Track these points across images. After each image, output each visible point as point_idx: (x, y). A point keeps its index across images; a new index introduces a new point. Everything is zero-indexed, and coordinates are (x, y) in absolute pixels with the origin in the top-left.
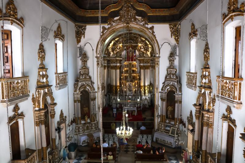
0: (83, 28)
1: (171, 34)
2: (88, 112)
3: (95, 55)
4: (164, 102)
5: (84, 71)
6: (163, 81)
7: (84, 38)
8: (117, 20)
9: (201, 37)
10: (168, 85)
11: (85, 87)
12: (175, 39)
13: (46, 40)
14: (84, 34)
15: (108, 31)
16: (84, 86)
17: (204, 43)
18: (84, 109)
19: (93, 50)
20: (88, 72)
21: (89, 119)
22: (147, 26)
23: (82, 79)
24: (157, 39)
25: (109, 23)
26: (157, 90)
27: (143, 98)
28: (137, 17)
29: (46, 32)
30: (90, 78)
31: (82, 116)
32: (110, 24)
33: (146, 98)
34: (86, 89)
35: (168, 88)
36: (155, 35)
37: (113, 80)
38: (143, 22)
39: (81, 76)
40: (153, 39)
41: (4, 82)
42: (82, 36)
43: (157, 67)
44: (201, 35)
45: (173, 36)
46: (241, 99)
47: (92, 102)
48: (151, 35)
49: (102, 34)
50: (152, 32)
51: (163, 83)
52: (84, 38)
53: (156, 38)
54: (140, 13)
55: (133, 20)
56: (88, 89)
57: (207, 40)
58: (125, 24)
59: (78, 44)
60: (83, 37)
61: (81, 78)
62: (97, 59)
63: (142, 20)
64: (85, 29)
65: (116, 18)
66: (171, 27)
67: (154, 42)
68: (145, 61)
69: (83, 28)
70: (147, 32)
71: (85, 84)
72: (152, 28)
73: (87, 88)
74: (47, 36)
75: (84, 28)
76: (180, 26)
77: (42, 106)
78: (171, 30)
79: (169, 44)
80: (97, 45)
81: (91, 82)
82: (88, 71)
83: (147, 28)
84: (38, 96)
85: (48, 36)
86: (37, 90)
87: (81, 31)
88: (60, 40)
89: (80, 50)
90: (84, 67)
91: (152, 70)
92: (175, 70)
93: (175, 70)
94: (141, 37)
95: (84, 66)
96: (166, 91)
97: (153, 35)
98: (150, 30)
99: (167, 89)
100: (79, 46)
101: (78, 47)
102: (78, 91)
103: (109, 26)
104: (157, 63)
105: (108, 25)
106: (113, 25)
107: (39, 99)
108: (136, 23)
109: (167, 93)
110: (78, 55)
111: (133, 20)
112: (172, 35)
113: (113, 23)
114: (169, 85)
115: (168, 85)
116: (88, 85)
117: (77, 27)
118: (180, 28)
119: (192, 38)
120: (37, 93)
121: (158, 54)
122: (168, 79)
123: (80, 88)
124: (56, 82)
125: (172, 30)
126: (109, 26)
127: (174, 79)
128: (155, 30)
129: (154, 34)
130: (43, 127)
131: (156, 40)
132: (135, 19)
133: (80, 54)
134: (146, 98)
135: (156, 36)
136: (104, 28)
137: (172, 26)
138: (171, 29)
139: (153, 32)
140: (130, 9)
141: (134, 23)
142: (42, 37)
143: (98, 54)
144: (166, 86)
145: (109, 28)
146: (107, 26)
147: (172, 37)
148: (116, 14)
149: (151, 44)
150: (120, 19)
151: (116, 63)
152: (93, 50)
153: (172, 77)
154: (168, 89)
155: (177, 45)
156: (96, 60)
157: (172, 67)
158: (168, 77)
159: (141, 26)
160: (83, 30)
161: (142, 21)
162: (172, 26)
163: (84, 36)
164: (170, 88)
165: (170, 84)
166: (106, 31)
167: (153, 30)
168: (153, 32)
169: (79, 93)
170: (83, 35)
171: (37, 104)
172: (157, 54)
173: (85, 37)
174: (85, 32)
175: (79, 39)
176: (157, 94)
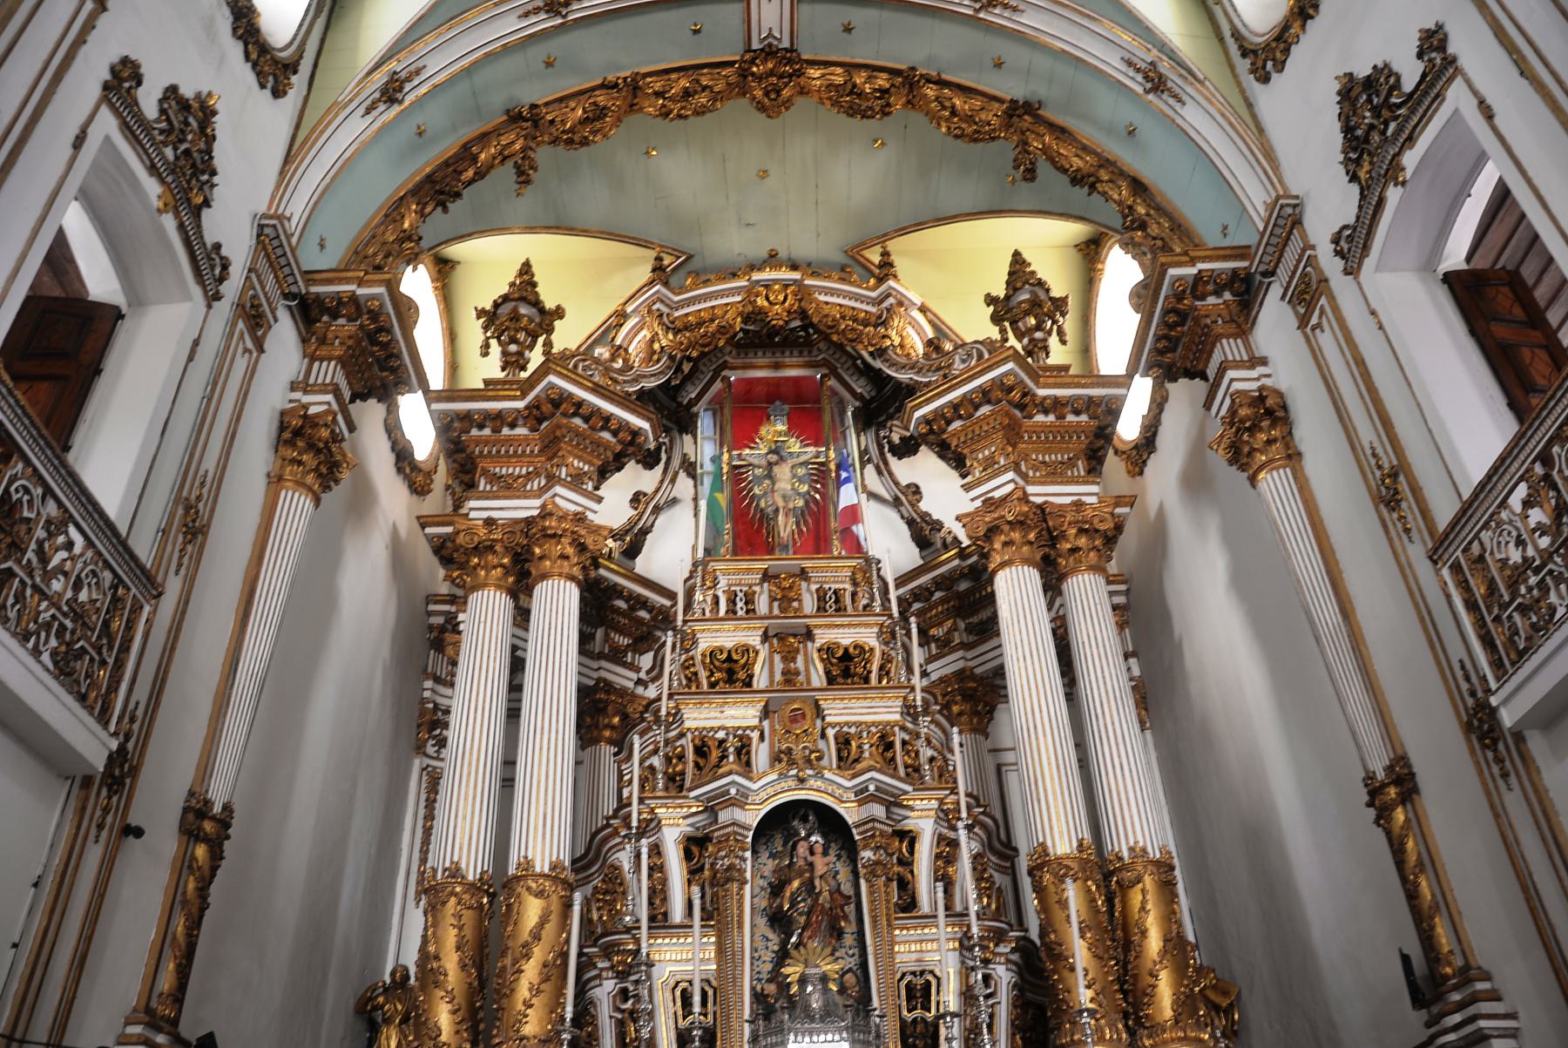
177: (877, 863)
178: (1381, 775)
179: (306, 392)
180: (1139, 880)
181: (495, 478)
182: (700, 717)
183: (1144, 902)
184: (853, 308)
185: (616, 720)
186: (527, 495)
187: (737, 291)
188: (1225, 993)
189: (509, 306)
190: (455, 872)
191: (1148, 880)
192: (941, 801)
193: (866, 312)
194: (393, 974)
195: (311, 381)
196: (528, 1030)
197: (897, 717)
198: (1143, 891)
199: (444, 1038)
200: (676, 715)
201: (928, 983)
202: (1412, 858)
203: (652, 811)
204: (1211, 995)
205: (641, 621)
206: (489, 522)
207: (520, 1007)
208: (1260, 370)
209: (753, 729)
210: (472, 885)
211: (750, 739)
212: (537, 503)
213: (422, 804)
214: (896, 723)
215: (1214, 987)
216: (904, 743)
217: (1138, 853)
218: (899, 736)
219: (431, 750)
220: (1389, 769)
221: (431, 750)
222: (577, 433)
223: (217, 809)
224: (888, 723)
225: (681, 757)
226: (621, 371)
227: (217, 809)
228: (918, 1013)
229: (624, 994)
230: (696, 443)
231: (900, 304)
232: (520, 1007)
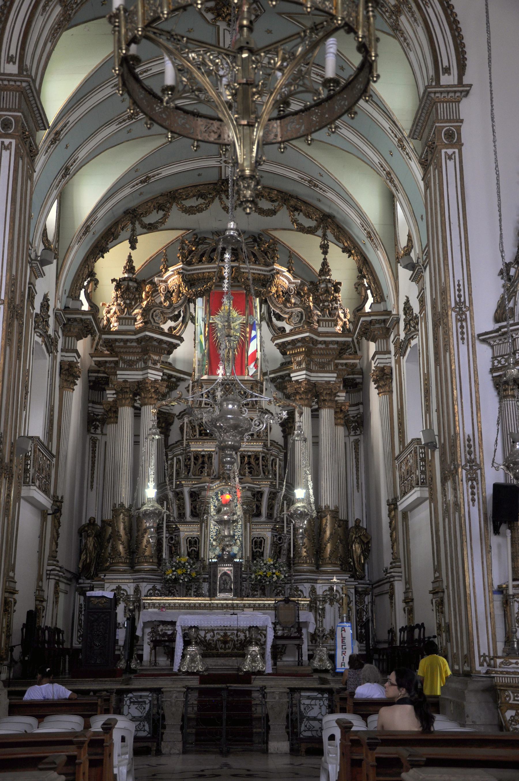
26: (461, 319)
27: (313, 590)
37: (116, 470)
43: (450, 158)
68: (317, 359)
91: (357, 443)
104: (450, 135)
121: (455, 70)
149: (356, 245)
151: (141, 364)
172: (447, 71)
176: (463, 348)
177: (248, 510)
178: (390, 501)
179: (66, 352)
180: (326, 516)
181: (124, 362)
182: (196, 447)
183: (326, 522)
184: (259, 274)
185: (163, 425)
186: (137, 370)
187: (214, 268)
188: (367, 538)
189: (126, 283)
190: (122, 505)
191: (328, 516)
192: (272, 482)
193: (264, 275)
194: (90, 520)
195: (67, 347)
196: (146, 554)
197: (260, 449)
198: (327, 519)
199: (122, 555)
200: (188, 445)
201: (261, 541)
202: (393, 526)
203: (180, 482)
204: (362, 537)
205: (173, 382)
206: (125, 381)
207: (144, 547)
208: (387, 356)
209: (213, 451)
210: (127, 509)
211: (212, 455)
212: (141, 373)
213: (91, 452)
214: (260, 452)
215: (364, 535)
216: (263, 457)
217: (327, 507)
218: (261, 455)
219: (92, 431)
220: (392, 500)
221: (92, 431)
222: (155, 347)
223: (60, 498)
224: (258, 451)
225: (189, 459)
226: (168, 308)
227: (60, 498)
228: (258, 549)
229: (172, 539)
230: (195, 308)
231: (278, 273)
232: (144, 547)
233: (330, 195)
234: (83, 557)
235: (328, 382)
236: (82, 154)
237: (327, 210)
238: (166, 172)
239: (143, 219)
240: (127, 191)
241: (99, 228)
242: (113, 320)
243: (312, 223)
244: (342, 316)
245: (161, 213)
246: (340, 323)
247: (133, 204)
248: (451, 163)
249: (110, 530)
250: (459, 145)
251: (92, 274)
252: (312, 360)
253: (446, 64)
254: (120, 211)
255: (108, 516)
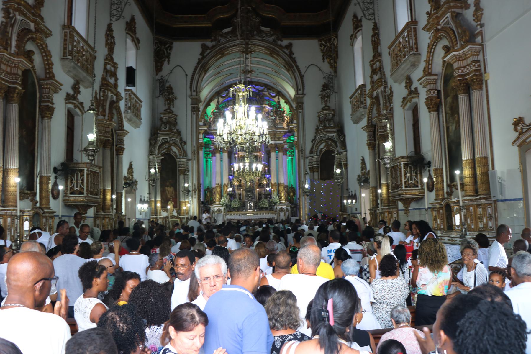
0: (168, 45)
1: (323, 56)
2: (173, 195)
3: (189, 93)
4: (316, 173)
5: (169, 117)
6: (313, 137)
7: (169, 63)
8: (227, 33)
9: (364, 15)
10: (322, 141)
11: (169, 149)
12: (330, 63)
13: (119, 19)
14: (168, 57)
15: (214, 51)
16: (166, 146)
17: (372, 26)
18: (166, 188)
19: (186, 75)
20: (175, 121)
21: (175, 211)
22: (279, 42)
23: (164, 131)
24: (298, 64)
25: (213, 38)
27: (276, 208)
28: (263, 28)
29: (119, 7)
30: (179, 133)
31: (163, 201)
32: (215, 40)
33: (282, 208)
34: (171, 151)
35: (322, 146)
36: (295, 58)
38: (273, 37)
39: (163, 125)
40: (291, 65)
41: (68, 31)
42: (165, 60)
43: (300, 112)
44: (364, 12)
45: (326, 60)
46: (419, 50)
47: (182, 176)
48: (287, 58)
49: (200, 57)
50: (288, 53)
51: (312, 142)
52: (169, 63)
53: (295, 62)
54: (267, 22)
55: (255, 32)
56: (175, 152)
57: (374, 19)
58: (242, 40)
59: (157, 74)
60: (166, 63)
61: (163, 129)
62: (192, 99)
63: (272, 33)
64: (171, 48)
65: (225, 30)
66: (322, 44)
67: (294, 70)
68: (277, 136)
69: (168, 45)
70: (281, 53)
71: (171, 140)
72: (290, 46)
73: (172, 150)
74: (121, 12)
75: (169, 47)
76: (336, 39)
77: (108, 117)
78: (322, 50)
79: (320, 69)
80: (192, 76)
81: (181, 140)
82: (176, 119)
83: (281, 47)
84: (102, 98)
85: (122, 13)
86: (103, 90)
87: (164, 51)
88: (133, 42)
89: (160, 83)
90: (168, 111)
91: (292, 159)
92: (332, 112)
93: (332, 112)
94: (269, 89)
95: (167, 109)
96: (318, 154)
97: (292, 57)
98: (285, 50)
99: (319, 149)
100: (158, 77)
101: (157, 80)
102: (157, 151)
103: (214, 43)
105: (211, 41)
106: (221, 41)
107: (105, 104)
108: (261, 39)
109: (321, 157)
110: (157, 93)
111: (255, 32)
112: (325, 58)
113: (220, 38)
114: (322, 140)
115: (322, 141)
116: (175, 144)
117: (156, 43)
118: (337, 44)
119: (355, 39)
120: (101, 93)
121: (302, 90)
122: (321, 129)
123: (160, 146)
124: (126, 105)
125: (324, 49)
126: (214, 43)
127: (332, 127)
128: (294, 49)
129: (294, 56)
130: (108, 151)
131: (297, 67)
132: (260, 32)
133: (160, 91)
134: (282, 208)
135: (296, 59)
136: (204, 48)
137: (323, 42)
138: (322, 48)
139: (290, 53)
140: (250, 14)
141: (257, 38)
142: (111, 15)
143: (194, 91)
144: (319, 142)
145: (213, 47)
146: (209, 44)
147: (324, 61)
148: (226, 23)
150: (233, 32)
152: (186, 75)
153: (327, 125)
154: (322, 149)
155: (333, 74)
156: (189, 101)
157: (327, 108)
158: (320, 128)
159: (270, 43)
160: (166, 49)
161: (272, 35)
162: (323, 42)
163: (169, 61)
164: (324, 147)
165: (325, 137)
166: (208, 51)
167: (291, 49)
168: (291, 53)
169: (158, 154)
170: (167, 60)
171: (101, 110)
172: (300, 90)
173: (170, 62)
174: (169, 54)
175: (159, 64)
233: (280, 87)
234: (206, 198)
235: (281, 144)
236: (204, 86)
237: (279, 90)
238: (228, 82)
239: (221, 94)
240: (216, 88)
241: (208, 99)
242: (212, 122)
243: (274, 95)
244: (286, 119)
245: (227, 92)
246: (286, 121)
247: (218, 90)
248: (300, 114)
249: (214, 190)
250: (302, 109)
251: (206, 113)
252: (276, 137)
253: (299, 88)
254: (214, 93)
255: (214, 186)
